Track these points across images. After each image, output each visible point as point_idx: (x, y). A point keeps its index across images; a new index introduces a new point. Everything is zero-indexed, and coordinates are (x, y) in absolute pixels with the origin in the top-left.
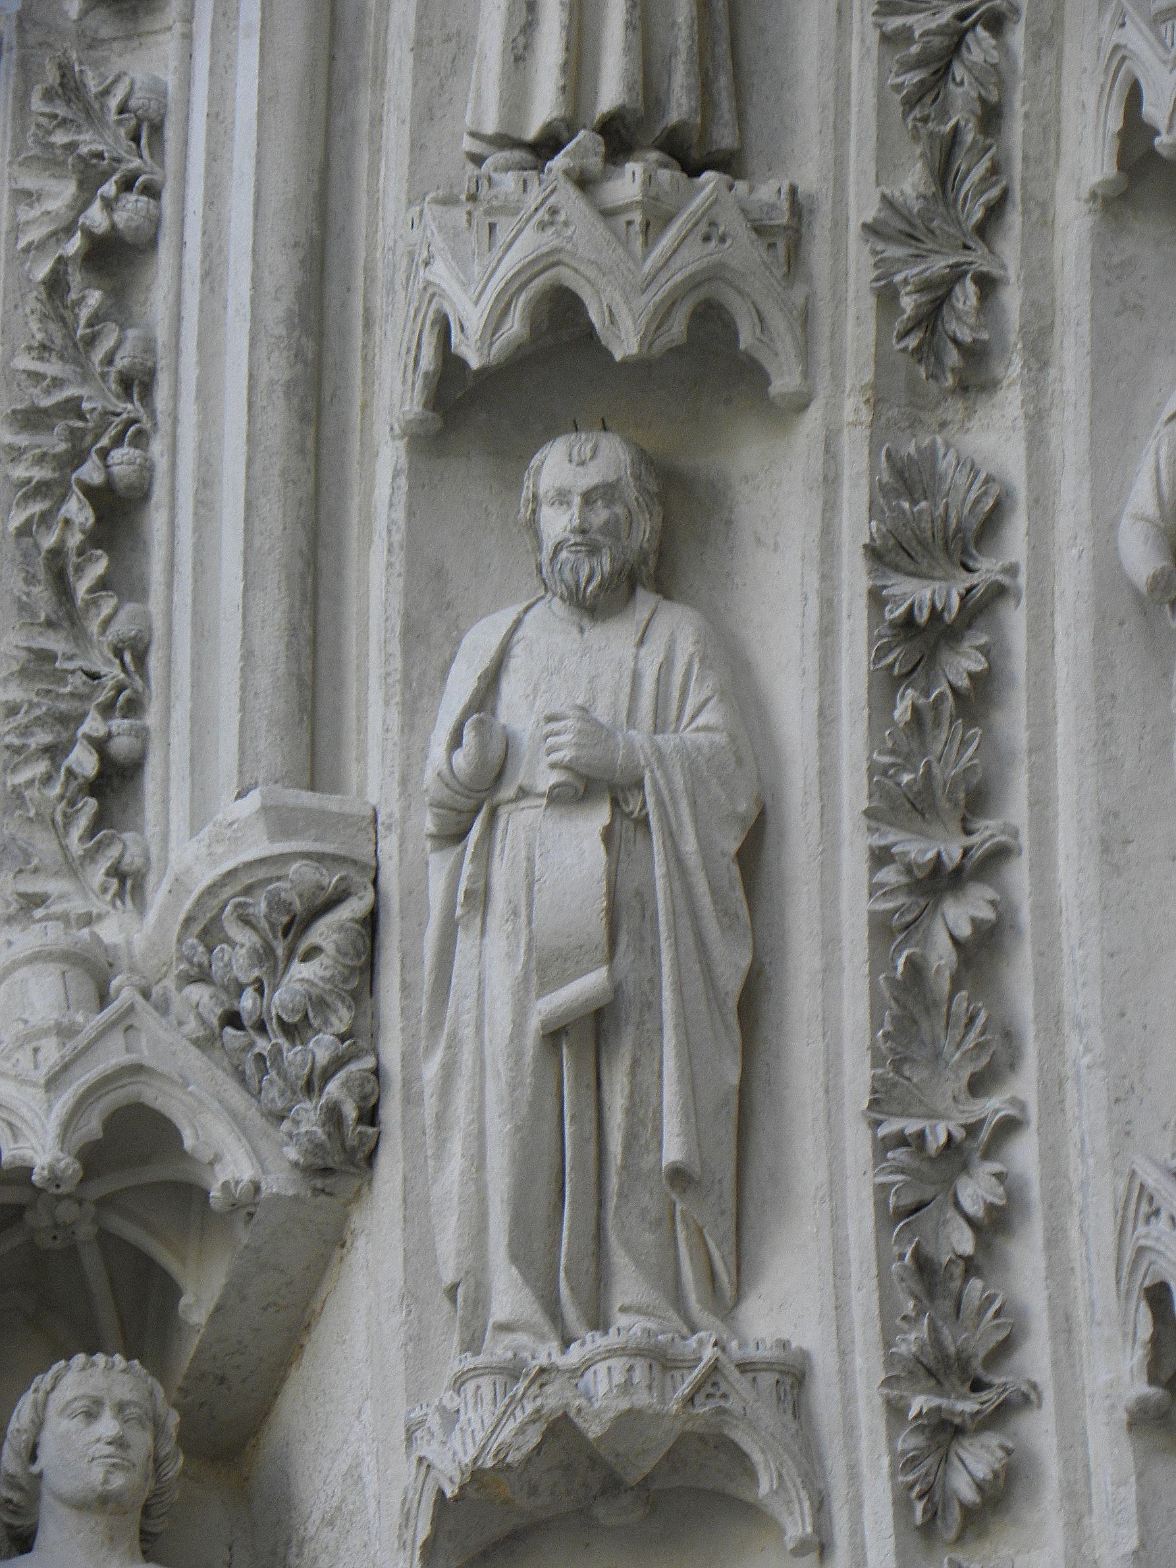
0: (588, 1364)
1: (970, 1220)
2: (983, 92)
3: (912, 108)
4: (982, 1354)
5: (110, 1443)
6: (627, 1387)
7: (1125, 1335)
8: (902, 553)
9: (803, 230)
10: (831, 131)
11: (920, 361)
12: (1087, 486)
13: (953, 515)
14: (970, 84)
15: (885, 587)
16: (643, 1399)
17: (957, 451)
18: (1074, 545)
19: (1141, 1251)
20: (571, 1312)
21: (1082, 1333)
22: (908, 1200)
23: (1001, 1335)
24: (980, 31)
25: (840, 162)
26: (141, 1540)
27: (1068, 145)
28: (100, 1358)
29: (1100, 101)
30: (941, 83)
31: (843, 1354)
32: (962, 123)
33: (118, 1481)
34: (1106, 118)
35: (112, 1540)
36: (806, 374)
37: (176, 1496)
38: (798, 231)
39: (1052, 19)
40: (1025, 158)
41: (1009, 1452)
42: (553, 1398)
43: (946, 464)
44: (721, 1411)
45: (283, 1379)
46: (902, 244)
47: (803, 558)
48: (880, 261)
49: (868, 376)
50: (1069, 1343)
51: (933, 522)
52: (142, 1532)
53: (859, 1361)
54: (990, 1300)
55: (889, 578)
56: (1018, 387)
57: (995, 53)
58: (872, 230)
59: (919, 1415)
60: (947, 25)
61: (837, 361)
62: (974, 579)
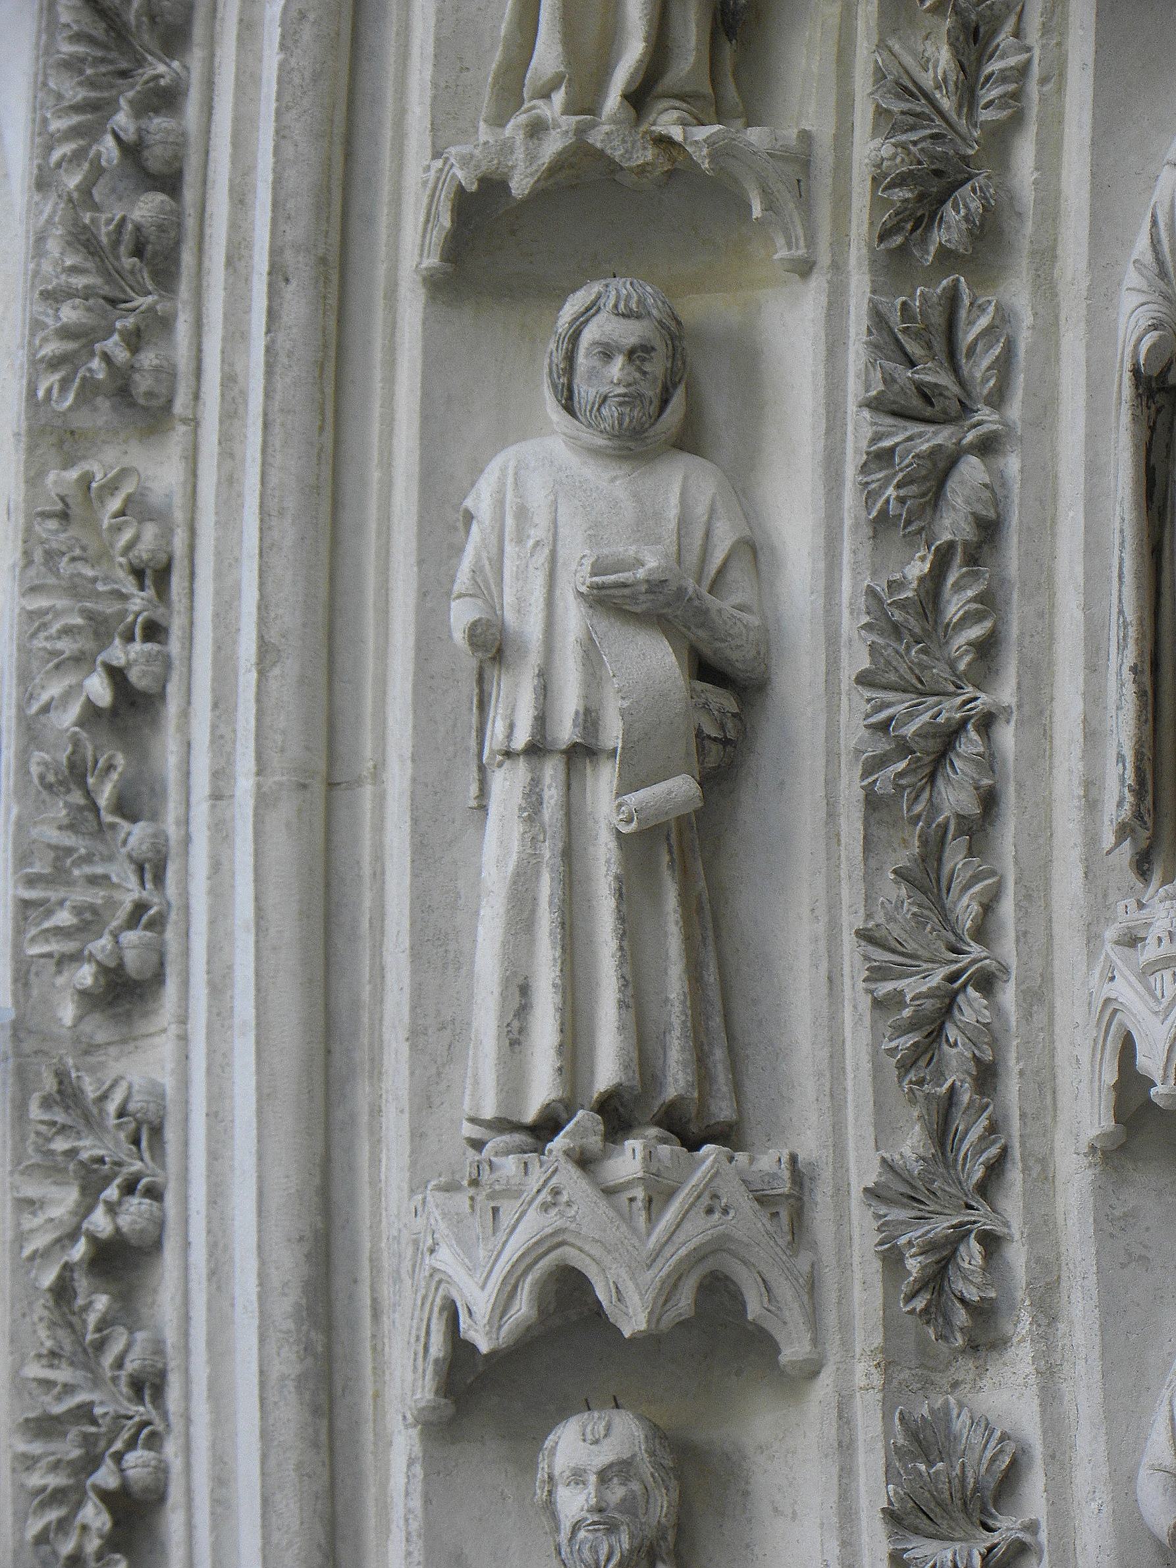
2: (976, 1052)
3: (907, 1071)
8: (921, 1515)
9: (805, 1198)
10: (827, 1099)
11: (928, 1322)
12: (1102, 1439)
13: (970, 1474)
14: (963, 1045)
15: (906, 1550)
17: (970, 1411)
18: (1093, 1500)
24: (970, 989)
25: (838, 1128)
27: (1064, 1100)
29: (1094, 1055)
30: (935, 1045)
32: (958, 1083)
34: (1100, 1072)
36: (815, 1342)
38: (800, 1199)
39: (1041, 975)
40: (1023, 1116)
43: (960, 1424)
46: (904, 1206)
47: (822, 1524)
48: (884, 1224)
49: (878, 1340)
51: (950, 1482)
55: (910, 1541)
56: (1028, 1344)
57: (987, 1013)
58: (873, 1194)
60: (938, 988)
61: (845, 1326)
62: (995, 1538)
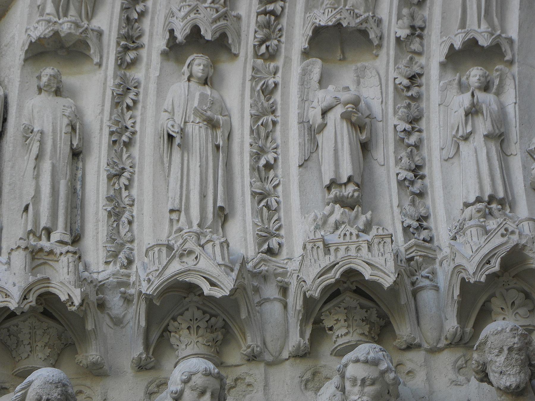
0: (63, 23)
1: (137, 12)
4: (136, 37)
6: (70, 28)
7: (163, 38)
16: (73, 31)
19: (170, 22)
20: (61, 14)
21: (154, 37)
22: (127, 6)
23: (139, 34)
31: (110, 32)
41: (137, 55)
42: (56, 27)
44: (87, 36)
50: (152, 38)
53: (113, 34)
54: (139, 27)
59: (123, 45)
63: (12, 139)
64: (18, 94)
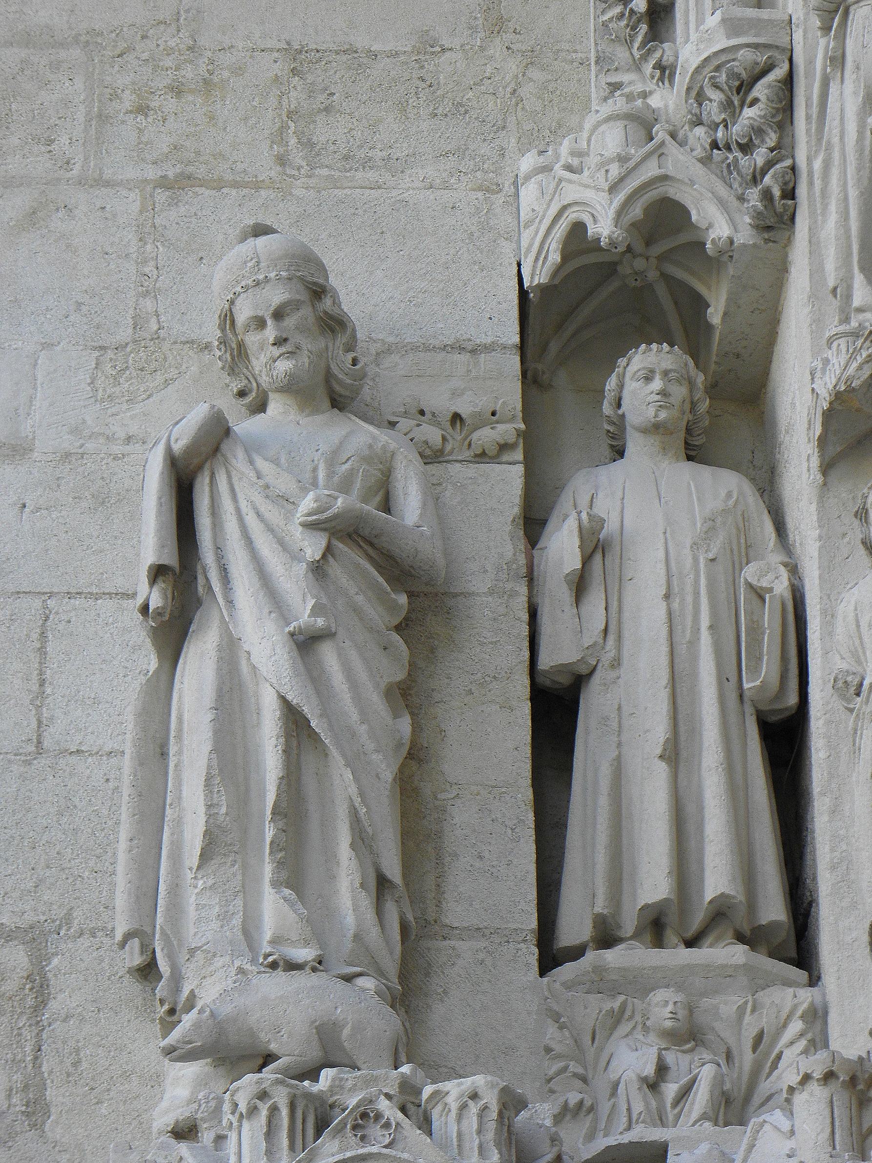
5: (658, 394)
26: (686, 449)
28: (654, 346)
33: (663, 415)
35: (664, 450)
37: (707, 423)
45: (772, 352)
52: (686, 443)
63: (821, 722)
64: (820, 577)
